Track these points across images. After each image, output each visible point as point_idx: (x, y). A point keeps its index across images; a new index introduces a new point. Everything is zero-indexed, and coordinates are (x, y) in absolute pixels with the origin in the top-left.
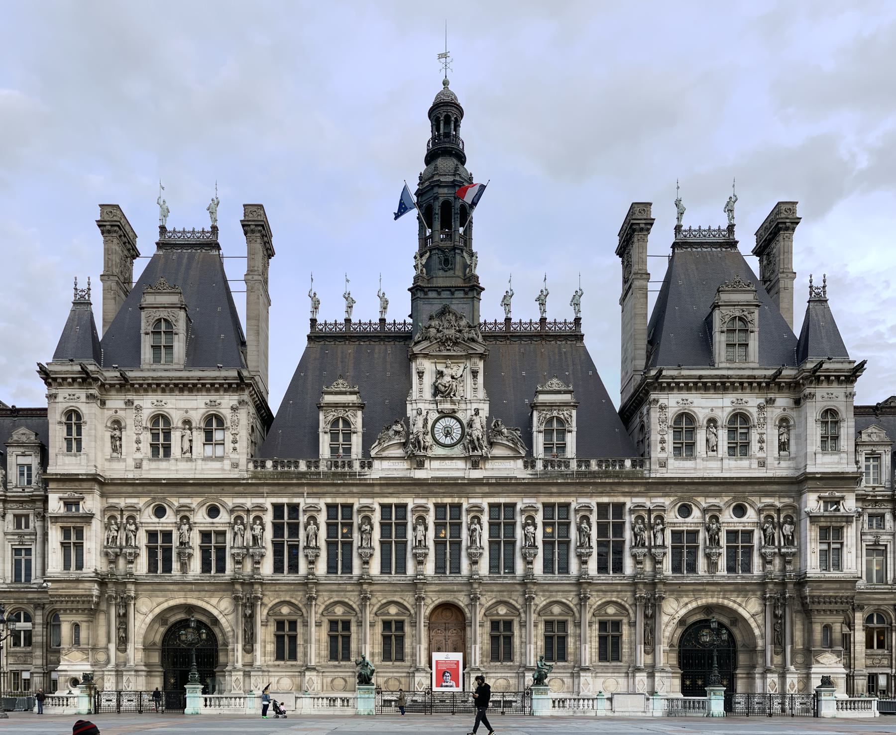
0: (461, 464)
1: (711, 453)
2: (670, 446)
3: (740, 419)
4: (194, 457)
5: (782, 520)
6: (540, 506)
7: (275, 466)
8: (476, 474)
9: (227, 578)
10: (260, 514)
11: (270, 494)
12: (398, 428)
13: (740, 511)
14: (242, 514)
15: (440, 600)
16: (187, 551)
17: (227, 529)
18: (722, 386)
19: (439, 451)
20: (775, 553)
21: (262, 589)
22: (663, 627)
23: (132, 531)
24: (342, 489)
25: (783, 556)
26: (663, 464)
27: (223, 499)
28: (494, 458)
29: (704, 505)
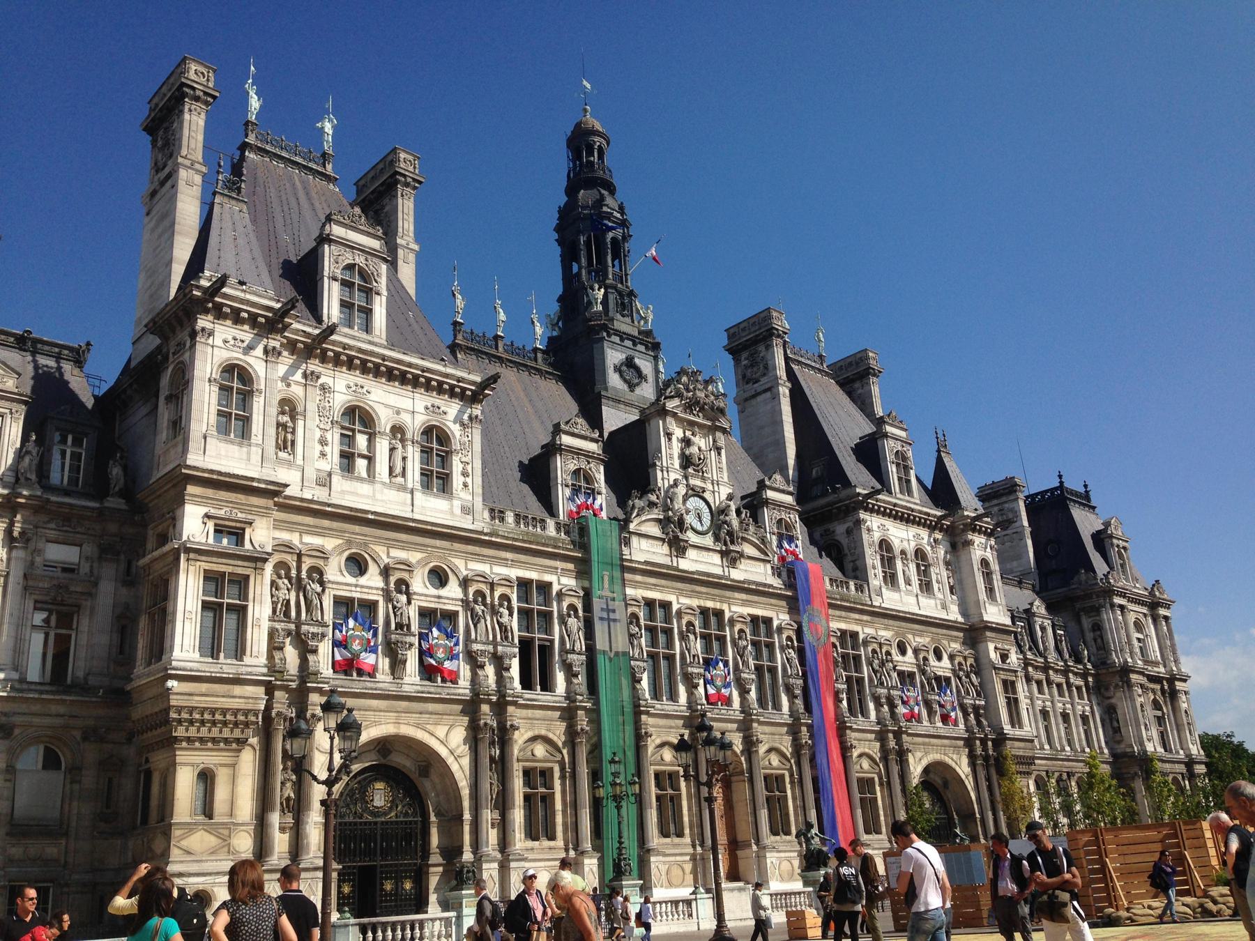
0: (716, 559)
2: (881, 575)
3: (920, 554)
4: (410, 485)
7: (518, 523)
8: (737, 574)
9: (461, 691)
10: (507, 591)
11: (514, 564)
12: (653, 498)
14: (485, 589)
16: (409, 639)
17: (460, 609)
18: (906, 518)
23: (318, 594)
25: (976, 709)
26: (880, 594)
27: (453, 560)
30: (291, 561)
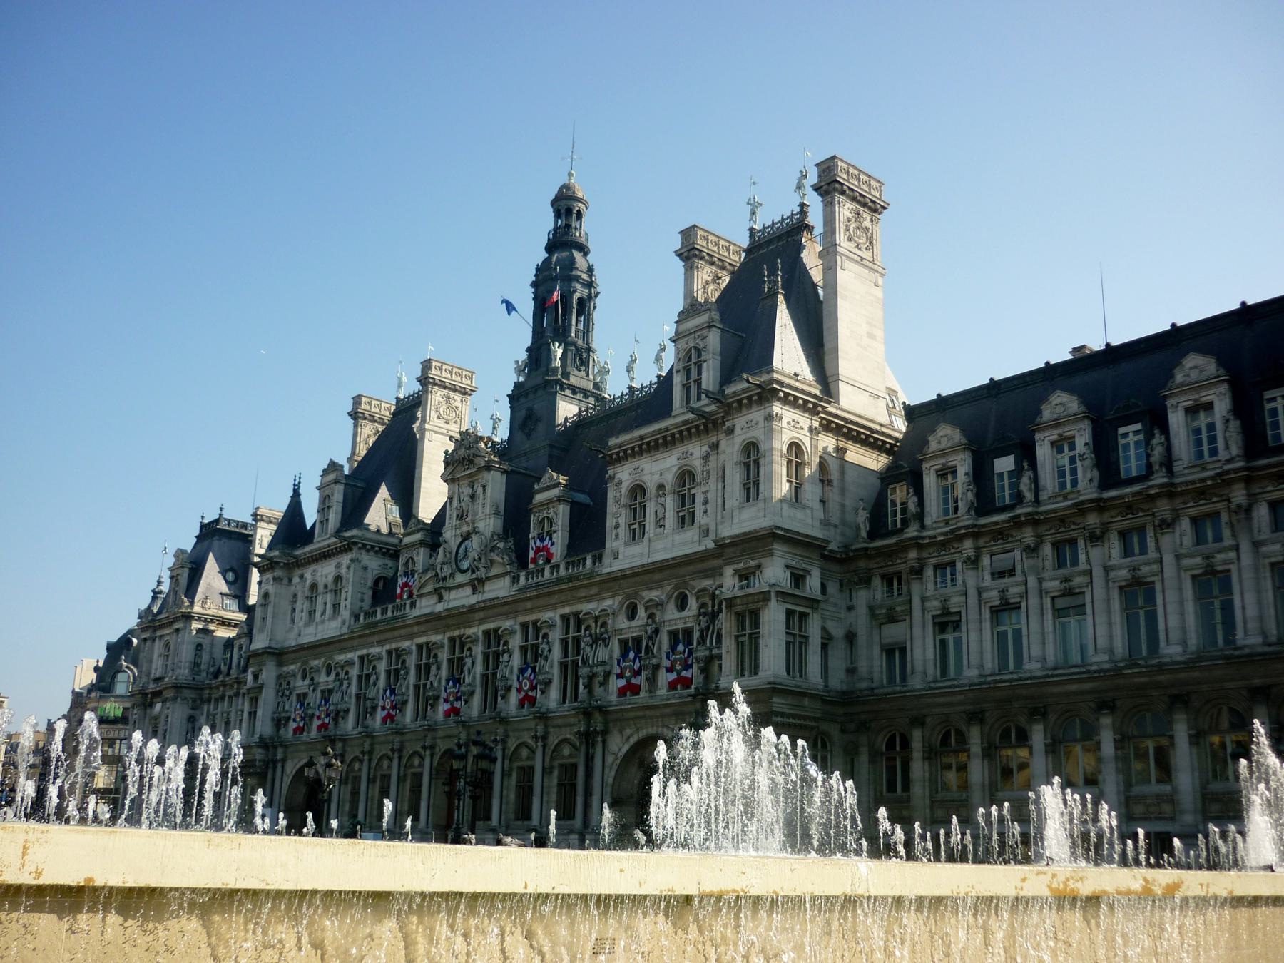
0: (468, 590)
1: (659, 530)
2: (623, 531)
3: (686, 476)
5: (716, 608)
6: (518, 627)
8: (473, 600)
11: (359, 647)
13: (682, 604)
14: (339, 670)
15: (446, 747)
19: (460, 578)
20: (706, 657)
21: (344, 746)
22: (607, 771)
24: (396, 633)
28: (488, 579)
29: (647, 599)
30: (282, 681)
